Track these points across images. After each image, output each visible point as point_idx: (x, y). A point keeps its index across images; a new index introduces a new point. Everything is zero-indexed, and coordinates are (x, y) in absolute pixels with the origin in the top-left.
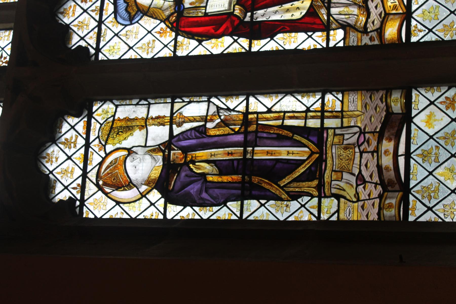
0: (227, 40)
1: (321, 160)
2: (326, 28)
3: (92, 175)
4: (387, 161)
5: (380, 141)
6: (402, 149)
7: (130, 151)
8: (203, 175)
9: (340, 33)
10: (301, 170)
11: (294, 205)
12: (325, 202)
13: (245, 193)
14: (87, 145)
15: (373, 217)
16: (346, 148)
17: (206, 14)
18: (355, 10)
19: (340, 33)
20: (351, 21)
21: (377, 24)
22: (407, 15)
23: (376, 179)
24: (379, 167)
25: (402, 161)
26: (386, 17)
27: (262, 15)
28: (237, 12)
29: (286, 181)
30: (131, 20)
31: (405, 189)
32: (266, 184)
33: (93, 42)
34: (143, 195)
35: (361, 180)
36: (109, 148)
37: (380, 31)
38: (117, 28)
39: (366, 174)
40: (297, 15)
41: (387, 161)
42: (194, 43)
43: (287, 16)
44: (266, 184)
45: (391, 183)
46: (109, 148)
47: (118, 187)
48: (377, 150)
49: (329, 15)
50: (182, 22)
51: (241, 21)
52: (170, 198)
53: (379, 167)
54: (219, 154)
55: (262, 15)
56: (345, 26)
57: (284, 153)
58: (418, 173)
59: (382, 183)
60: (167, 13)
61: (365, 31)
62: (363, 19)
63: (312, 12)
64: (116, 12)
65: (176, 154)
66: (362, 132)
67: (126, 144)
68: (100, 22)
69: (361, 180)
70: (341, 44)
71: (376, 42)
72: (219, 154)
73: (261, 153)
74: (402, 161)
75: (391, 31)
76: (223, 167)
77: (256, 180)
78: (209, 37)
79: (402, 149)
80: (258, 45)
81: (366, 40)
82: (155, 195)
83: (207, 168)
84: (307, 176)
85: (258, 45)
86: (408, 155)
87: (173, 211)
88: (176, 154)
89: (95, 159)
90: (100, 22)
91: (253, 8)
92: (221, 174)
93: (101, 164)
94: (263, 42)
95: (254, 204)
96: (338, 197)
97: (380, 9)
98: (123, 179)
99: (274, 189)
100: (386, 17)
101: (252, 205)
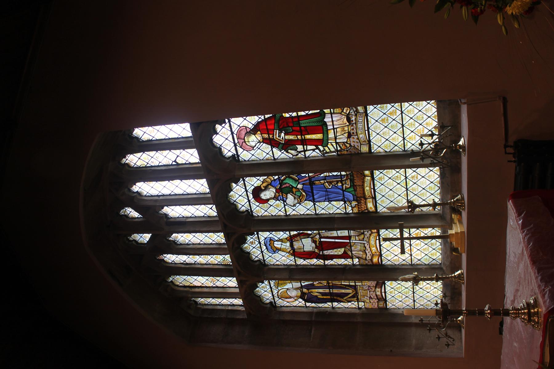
0: (315, 260)
1: (357, 293)
2: (352, 258)
3: (276, 295)
4: (378, 293)
5: (375, 288)
6: (383, 291)
7: (287, 289)
8: (316, 296)
9: (357, 260)
10: (350, 295)
11: (350, 304)
12: (360, 303)
13: (332, 301)
14: (271, 288)
15: (376, 306)
16: (365, 290)
17: (304, 251)
18: (361, 253)
19: (357, 260)
20: (360, 256)
21: (370, 258)
22: (381, 255)
23: (375, 297)
24: (376, 295)
25: (383, 294)
26: (373, 256)
27: (326, 252)
28: (316, 251)
29: (346, 298)
30: (275, 252)
31: (385, 301)
32: (339, 298)
33: (261, 258)
34: (296, 300)
35: (370, 298)
36: (279, 288)
37: (371, 260)
38: (270, 254)
39: (372, 297)
40: (340, 253)
41: (378, 293)
42: (302, 260)
43: (336, 253)
44: (339, 298)
45: (380, 298)
46: (279, 288)
47: (287, 298)
48: (375, 291)
49: (352, 254)
50: (295, 253)
51: (319, 254)
52: (306, 301)
53: (376, 295)
54: (321, 291)
55: (326, 252)
56: (358, 258)
57: (343, 291)
58: (389, 297)
59: (378, 299)
60: (289, 250)
61: (366, 259)
62: (364, 256)
63: (345, 252)
64: (267, 248)
65: (305, 290)
66: (369, 286)
67: (284, 287)
68: (262, 252)
69: (370, 298)
70: (358, 263)
71: (371, 263)
72: (321, 291)
73: (335, 291)
74: (383, 294)
75: (375, 260)
76: (323, 294)
77: (335, 298)
78: (307, 259)
79: (383, 291)
80: (327, 262)
81: (367, 262)
82: (300, 300)
83: (317, 294)
84: (353, 297)
85: (327, 262)
86: (385, 292)
87: (308, 304)
88: (305, 290)
89: (275, 292)
90: (262, 252)
91: (323, 250)
92: (322, 296)
93: (278, 292)
94: (329, 261)
95: (336, 303)
96: (364, 302)
97: (370, 253)
98: (287, 296)
99: (342, 300)
100: (373, 256)
101: (335, 304)
